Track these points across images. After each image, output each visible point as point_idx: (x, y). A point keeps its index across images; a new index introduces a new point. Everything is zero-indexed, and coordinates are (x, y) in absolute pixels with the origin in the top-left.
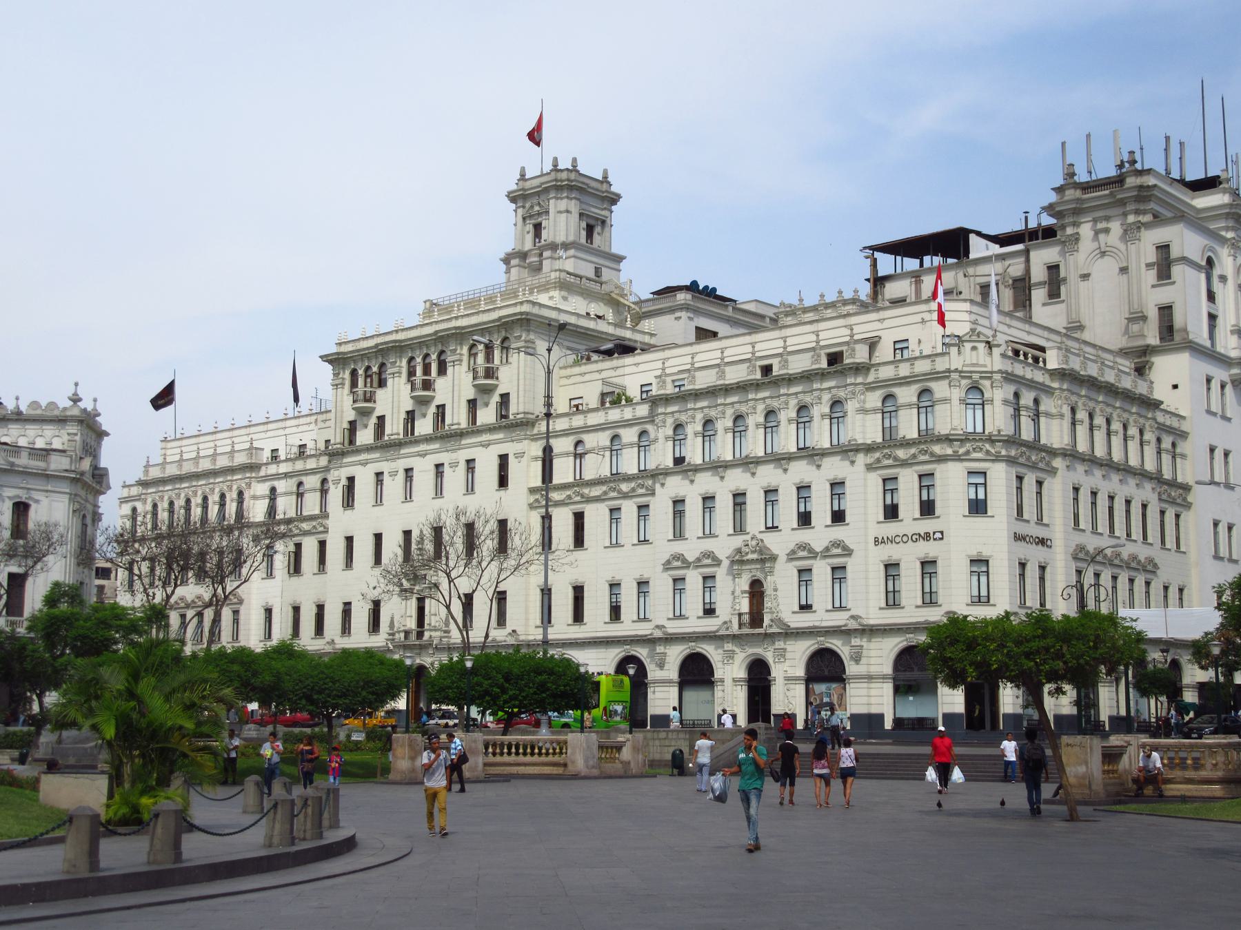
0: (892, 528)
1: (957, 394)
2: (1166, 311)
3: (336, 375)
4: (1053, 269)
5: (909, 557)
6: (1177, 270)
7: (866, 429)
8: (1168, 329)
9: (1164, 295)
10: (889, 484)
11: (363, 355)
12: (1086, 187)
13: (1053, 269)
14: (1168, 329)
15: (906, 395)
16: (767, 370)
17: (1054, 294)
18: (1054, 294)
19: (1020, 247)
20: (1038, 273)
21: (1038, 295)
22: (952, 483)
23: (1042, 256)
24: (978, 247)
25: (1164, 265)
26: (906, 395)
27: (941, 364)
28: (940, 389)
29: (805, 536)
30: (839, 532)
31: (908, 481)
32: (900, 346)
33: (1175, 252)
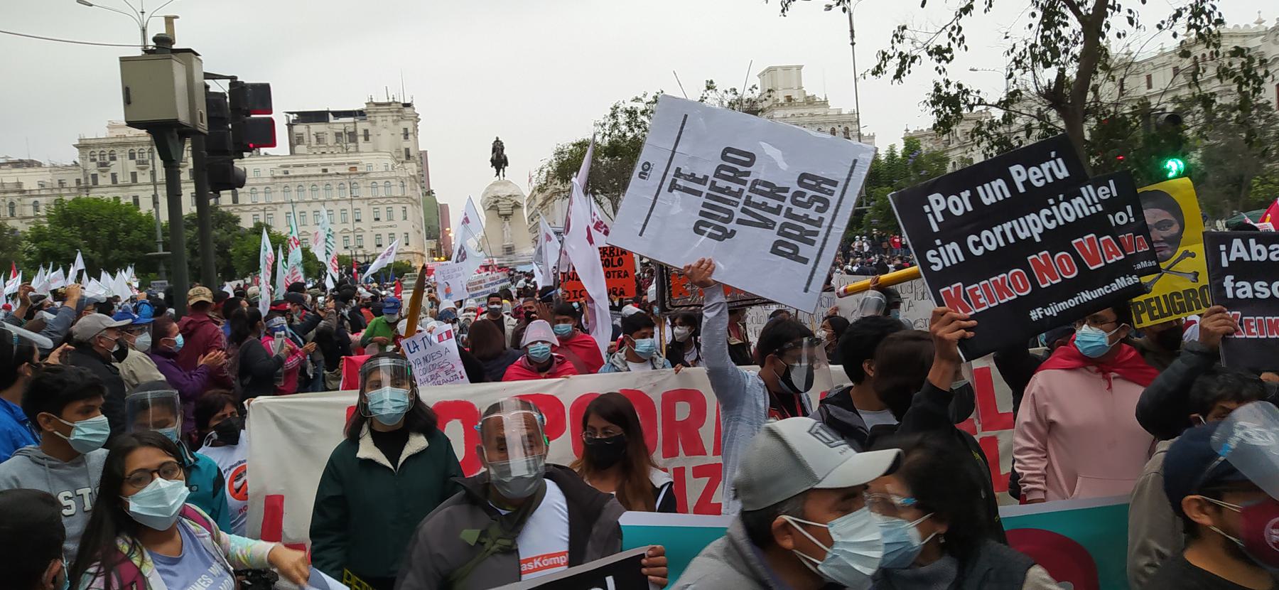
0: (377, 223)
1: (399, 183)
2: (407, 150)
3: (81, 153)
4: (366, 131)
5: (384, 233)
6: (410, 137)
7: (364, 192)
8: (408, 156)
9: (406, 144)
10: (376, 211)
11: (100, 145)
12: (377, 104)
13: (366, 131)
14: (408, 156)
15: (381, 183)
16: (325, 170)
17: (367, 139)
18: (367, 139)
19: (351, 119)
20: (360, 132)
21: (361, 139)
22: (397, 210)
23: (361, 126)
24: (331, 116)
25: (406, 135)
26: (381, 183)
27: (393, 174)
28: (393, 182)
29: (345, 226)
30: (357, 225)
31: (383, 209)
32: (370, 166)
33: (410, 130)
